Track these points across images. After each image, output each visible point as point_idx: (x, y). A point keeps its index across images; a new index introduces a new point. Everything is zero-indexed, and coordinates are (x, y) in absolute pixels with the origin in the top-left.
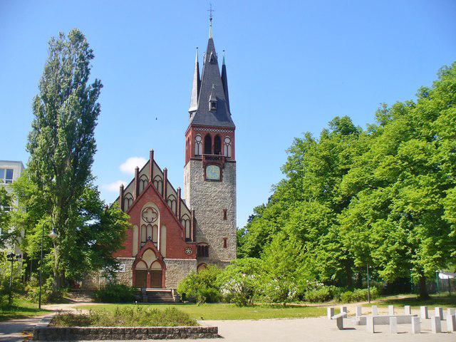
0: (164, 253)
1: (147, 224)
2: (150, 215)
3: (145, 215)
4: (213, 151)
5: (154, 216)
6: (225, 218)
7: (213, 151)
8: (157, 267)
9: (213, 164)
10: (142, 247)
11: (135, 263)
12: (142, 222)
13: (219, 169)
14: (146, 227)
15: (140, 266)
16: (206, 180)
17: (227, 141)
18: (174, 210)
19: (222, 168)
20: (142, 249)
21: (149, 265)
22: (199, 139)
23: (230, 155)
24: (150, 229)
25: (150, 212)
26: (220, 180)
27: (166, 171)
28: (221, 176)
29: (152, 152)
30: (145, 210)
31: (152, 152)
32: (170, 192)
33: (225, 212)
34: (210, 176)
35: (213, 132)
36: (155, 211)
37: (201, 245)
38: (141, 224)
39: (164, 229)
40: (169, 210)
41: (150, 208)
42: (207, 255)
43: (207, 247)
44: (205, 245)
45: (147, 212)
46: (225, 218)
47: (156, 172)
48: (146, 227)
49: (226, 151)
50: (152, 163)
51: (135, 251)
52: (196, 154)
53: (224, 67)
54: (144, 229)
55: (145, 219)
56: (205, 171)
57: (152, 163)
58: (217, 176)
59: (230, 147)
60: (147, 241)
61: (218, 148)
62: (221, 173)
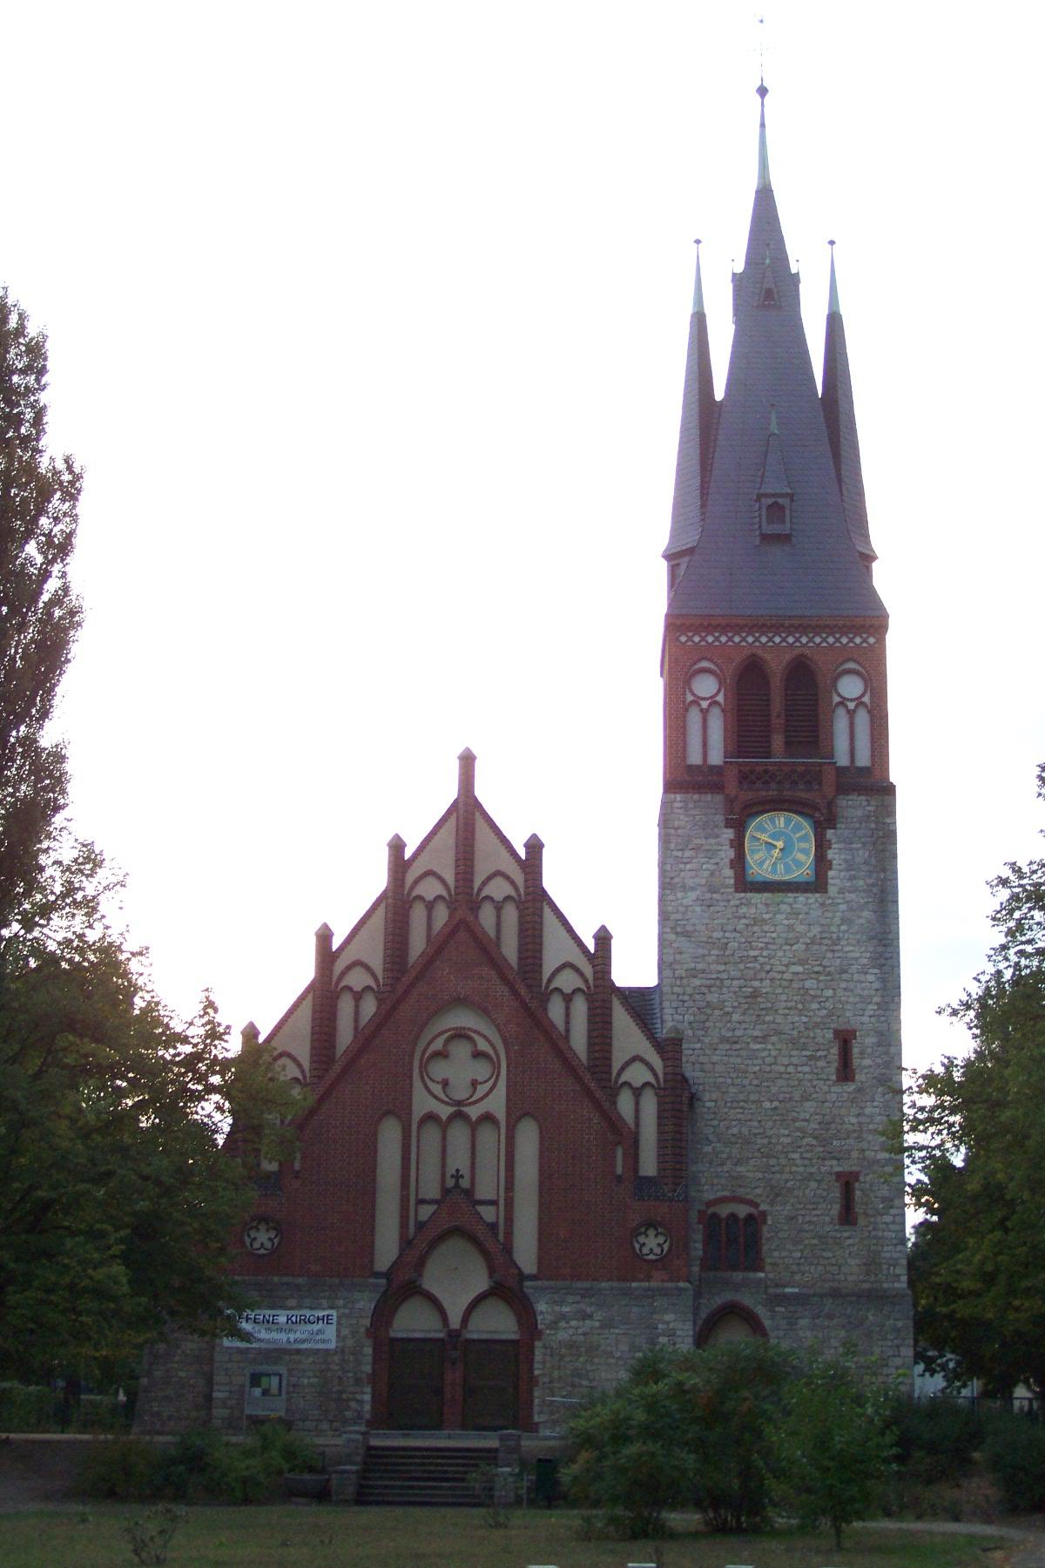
0: (526, 1253)
1: (445, 1112)
2: (460, 1070)
3: (439, 1070)
4: (778, 741)
5: (481, 1070)
6: (846, 1071)
7: (778, 741)
8: (498, 1323)
10: (421, 1226)
11: (383, 1314)
12: (422, 1103)
13: (807, 828)
15: (412, 1322)
16: (745, 884)
17: (850, 687)
18: (579, 1041)
19: (824, 820)
21: (455, 1322)
22: (706, 686)
24: (459, 1134)
26: (818, 884)
28: (822, 863)
29: (467, 762)
30: (438, 1045)
31: (467, 762)
32: (554, 953)
34: (762, 864)
35: (777, 649)
36: (483, 1045)
37: (724, 1211)
39: (528, 1139)
41: (460, 1035)
44: (742, 1211)
46: (846, 1071)
49: (846, 742)
51: (387, 1249)
52: (695, 758)
55: (437, 1089)
56: (738, 845)
58: (802, 864)
59: (862, 718)
60: (446, 1192)
62: (822, 846)
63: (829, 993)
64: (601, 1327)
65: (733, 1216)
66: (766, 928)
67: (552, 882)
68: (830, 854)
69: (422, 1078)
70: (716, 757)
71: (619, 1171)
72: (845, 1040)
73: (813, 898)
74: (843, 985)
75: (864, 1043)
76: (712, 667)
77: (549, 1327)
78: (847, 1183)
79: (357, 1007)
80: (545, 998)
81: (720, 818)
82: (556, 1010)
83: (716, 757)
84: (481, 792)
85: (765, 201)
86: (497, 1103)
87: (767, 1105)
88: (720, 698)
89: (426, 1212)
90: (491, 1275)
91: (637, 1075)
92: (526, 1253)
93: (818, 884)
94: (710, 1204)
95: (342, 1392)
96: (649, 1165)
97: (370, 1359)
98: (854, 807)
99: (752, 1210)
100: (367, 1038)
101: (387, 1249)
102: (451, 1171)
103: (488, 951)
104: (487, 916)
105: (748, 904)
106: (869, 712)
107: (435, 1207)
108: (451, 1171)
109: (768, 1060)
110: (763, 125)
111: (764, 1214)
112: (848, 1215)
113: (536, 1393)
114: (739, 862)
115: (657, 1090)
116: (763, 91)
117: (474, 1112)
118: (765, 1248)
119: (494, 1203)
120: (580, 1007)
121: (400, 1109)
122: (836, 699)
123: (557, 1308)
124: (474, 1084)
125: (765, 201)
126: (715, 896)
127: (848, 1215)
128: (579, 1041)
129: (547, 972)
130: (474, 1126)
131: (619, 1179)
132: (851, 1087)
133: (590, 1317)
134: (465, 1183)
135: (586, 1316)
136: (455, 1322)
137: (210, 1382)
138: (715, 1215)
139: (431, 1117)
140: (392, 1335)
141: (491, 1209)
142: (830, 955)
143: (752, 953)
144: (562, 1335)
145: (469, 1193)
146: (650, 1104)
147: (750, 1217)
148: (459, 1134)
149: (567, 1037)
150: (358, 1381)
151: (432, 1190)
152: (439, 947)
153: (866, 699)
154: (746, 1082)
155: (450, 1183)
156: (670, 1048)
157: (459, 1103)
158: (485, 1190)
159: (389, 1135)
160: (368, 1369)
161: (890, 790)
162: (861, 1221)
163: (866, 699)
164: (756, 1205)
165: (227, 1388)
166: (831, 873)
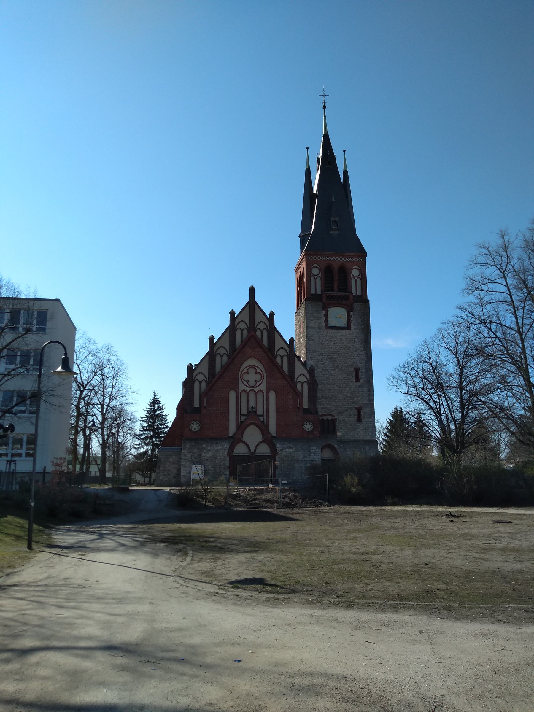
0: (272, 429)
1: (248, 389)
2: (252, 377)
3: (246, 377)
4: (336, 288)
5: (258, 377)
6: (357, 379)
7: (336, 288)
8: (264, 449)
9: (334, 305)
10: (242, 422)
12: (242, 387)
14: (248, 393)
15: (240, 450)
16: (328, 327)
17: (355, 273)
18: (285, 368)
20: (241, 427)
21: (252, 450)
22: (315, 271)
23: (359, 293)
24: (252, 396)
25: (252, 371)
26: (348, 327)
27: (272, 314)
28: (349, 321)
29: (252, 290)
30: (246, 370)
31: (252, 290)
32: (278, 345)
33: (357, 370)
34: (333, 322)
35: (336, 260)
36: (258, 370)
37: (325, 418)
38: (240, 390)
39: (272, 396)
40: (280, 369)
41: (252, 367)
42: (334, 432)
43: (334, 421)
44: (330, 418)
45: (247, 373)
46: (357, 379)
47: (258, 318)
48: (248, 393)
49: (354, 288)
50: (252, 304)
51: (232, 429)
52: (313, 292)
53: (346, 173)
54: (244, 396)
55: (246, 383)
56: (326, 316)
57: (252, 304)
58: (343, 322)
59: (359, 281)
60: (249, 412)
61: (345, 285)
63: (352, 357)
64: (295, 451)
65: (327, 419)
66: (335, 339)
67: (277, 325)
68: (352, 319)
69: (242, 381)
70: (319, 292)
71: (298, 406)
72: (357, 370)
73: (347, 331)
74: (356, 355)
75: (362, 371)
76: (317, 266)
77: (280, 451)
78: (359, 410)
79: (222, 359)
80: (275, 357)
81: (321, 308)
82: (279, 360)
83: (319, 292)
84: (258, 299)
85: (326, 138)
86: (263, 387)
87: (336, 388)
88: (320, 275)
89: (243, 418)
90: (263, 437)
91: (302, 379)
92: (272, 429)
93: (348, 327)
94: (321, 416)
95: (220, 472)
96: (306, 405)
97: (228, 462)
98: (357, 306)
99: (333, 418)
100: (225, 368)
101: (232, 429)
102: (250, 406)
103: (259, 343)
104: (258, 333)
105: (329, 333)
106: (361, 280)
107: (246, 417)
108: (250, 406)
109: (336, 376)
110: (325, 116)
111: (336, 419)
112: (359, 420)
113: (277, 471)
114: (326, 321)
115: (308, 383)
116: (325, 107)
117: (256, 389)
118: (337, 428)
119: (263, 415)
120: (285, 360)
121: (236, 390)
122: (352, 276)
123: (282, 446)
124: (256, 381)
125: (326, 138)
126: (321, 330)
127: (359, 420)
128: (285, 368)
129: (276, 349)
130: (256, 394)
131: (299, 408)
132: (358, 384)
133: (292, 448)
134: (254, 410)
135: (290, 448)
136: (252, 450)
137: (179, 470)
138: (323, 419)
139: (244, 390)
140: (234, 455)
141: (263, 417)
142: (352, 347)
143: (330, 346)
144: (284, 454)
145: (256, 412)
146: (306, 386)
147: (332, 419)
148: (252, 396)
149: (282, 367)
150: (225, 469)
151: (244, 411)
152: (245, 343)
153: (360, 276)
154: (330, 382)
155: (250, 410)
156: (311, 372)
157: (252, 387)
158: (260, 411)
159: (232, 395)
160: (228, 465)
161: (368, 301)
162: (363, 420)
163: (360, 276)
164: (334, 416)
165: (185, 472)
166: (352, 324)
